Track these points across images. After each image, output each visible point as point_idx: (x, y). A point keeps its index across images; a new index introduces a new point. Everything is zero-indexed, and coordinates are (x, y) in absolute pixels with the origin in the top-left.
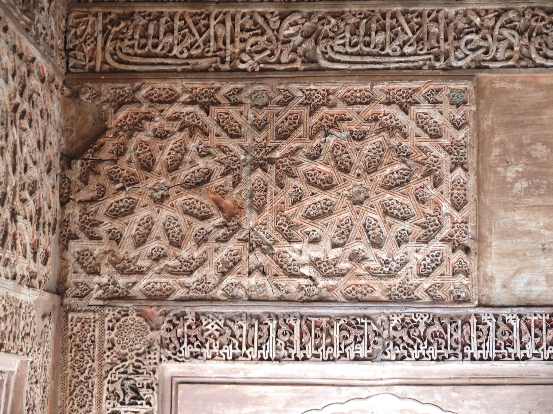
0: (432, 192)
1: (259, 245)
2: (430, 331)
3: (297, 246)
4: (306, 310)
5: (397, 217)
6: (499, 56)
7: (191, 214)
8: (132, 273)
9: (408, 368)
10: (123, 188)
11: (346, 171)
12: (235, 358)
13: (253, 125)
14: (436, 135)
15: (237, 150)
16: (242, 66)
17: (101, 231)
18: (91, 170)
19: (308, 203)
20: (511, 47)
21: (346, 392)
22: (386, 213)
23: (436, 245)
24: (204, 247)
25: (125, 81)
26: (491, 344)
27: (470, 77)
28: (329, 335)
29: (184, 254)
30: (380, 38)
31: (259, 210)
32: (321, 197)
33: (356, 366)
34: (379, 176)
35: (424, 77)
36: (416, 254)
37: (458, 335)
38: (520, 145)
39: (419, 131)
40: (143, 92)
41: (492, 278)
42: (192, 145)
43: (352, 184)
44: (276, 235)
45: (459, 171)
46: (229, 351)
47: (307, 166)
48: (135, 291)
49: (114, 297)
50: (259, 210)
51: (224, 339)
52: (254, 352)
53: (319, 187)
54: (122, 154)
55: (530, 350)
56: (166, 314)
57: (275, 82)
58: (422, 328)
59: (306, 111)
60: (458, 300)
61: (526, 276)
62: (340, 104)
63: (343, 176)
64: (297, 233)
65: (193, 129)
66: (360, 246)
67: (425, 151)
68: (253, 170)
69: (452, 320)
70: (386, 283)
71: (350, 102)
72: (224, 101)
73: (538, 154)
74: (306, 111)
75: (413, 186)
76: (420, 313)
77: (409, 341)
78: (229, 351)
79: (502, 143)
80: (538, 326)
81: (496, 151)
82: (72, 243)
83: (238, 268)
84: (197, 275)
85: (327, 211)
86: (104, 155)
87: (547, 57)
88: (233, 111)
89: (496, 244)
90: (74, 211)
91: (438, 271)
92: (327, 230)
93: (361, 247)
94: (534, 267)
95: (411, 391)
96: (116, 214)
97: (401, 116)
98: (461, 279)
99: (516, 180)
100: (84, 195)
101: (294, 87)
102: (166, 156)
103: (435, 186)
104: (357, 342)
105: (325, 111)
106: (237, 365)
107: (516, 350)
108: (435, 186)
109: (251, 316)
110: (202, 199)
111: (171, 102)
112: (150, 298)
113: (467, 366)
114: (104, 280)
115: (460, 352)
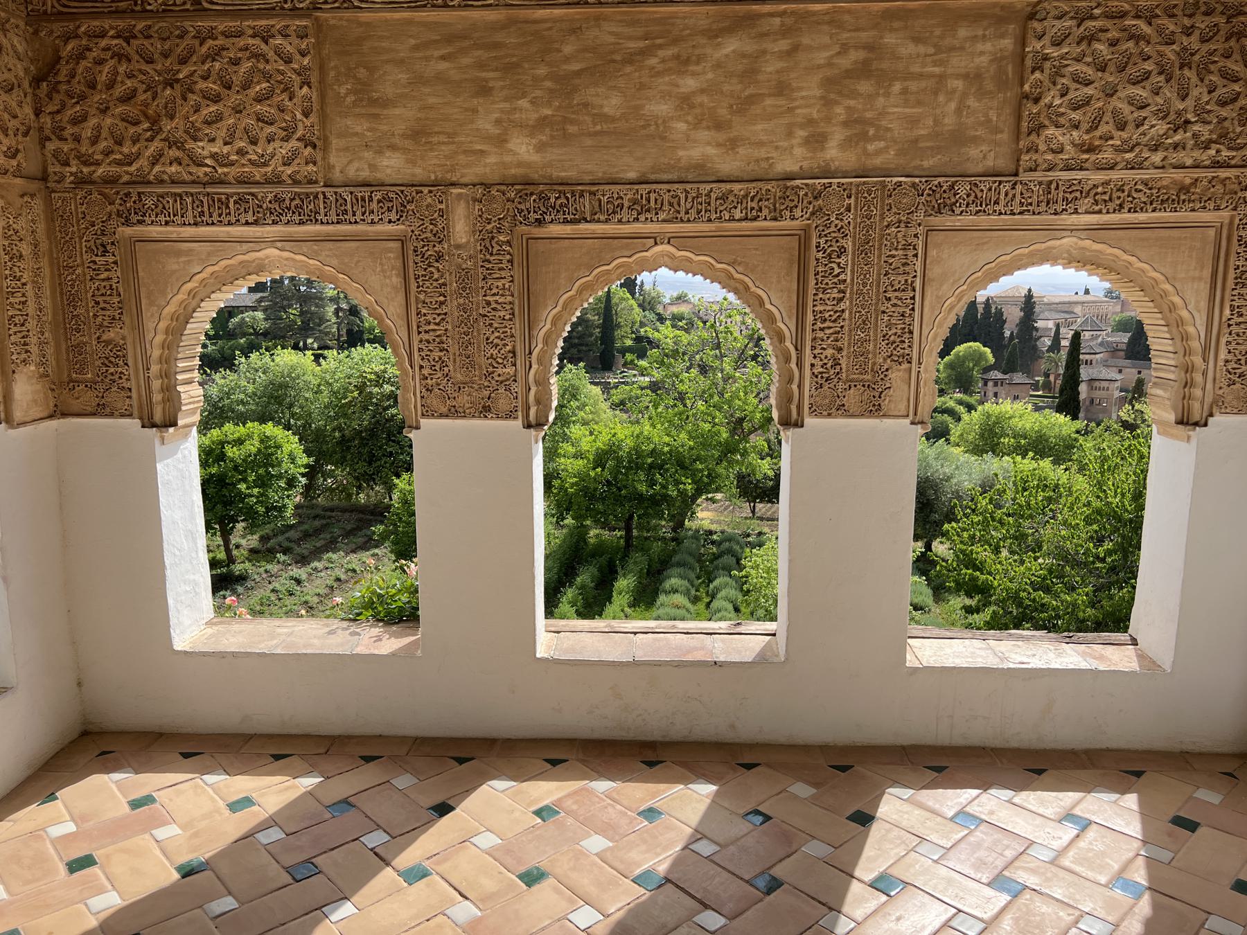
1: (175, 143)
2: (294, 203)
3: (201, 144)
5: (267, 123)
7: (127, 121)
8: (92, 164)
10: (77, 103)
11: (229, 88)
12: (167, 223)
13: (161, 54)
14: (288, 61)
16: (149, 8)
17: (66, 133)
18: (54, 89)
19: (205, 112)
21: (245, 247)
22: (258, 120)
23: (294, 143)
25: (69, 21)
26: (333, 212)
27: (309, 16)
28: (228, 207)
29: (126, 150)
31: (172, 118)
32: (213, 108)
33: (246, 228)
35: (277, 16)
36: (284, 150)
37: (312, 206)
38: (349, 69)
39: (277, 58)
40: (83, 29)
41: (334, 166)
42: (121, 69)
43: (234, 98)
44: (184, 135)
45: (305, 89)
46: (162, 219)
47: (202, 85)
49: (81, 182)
50: (172, 118)
51: (158, 210)
52: (178, 219)
53: (212, 100)
54: (73, 77)
55: (358, 217)
56: (118, 193)
57: (173, 20)
58: (287, 202)
59: (197, 42)
60: (310, 182)
61: (356, 165)
63: (227, 92)
64: (200, 134)
65: (121, 57)
67: (282, 73)
68: (165, 88)
69: (307, 195)
70: (263, 170)
71: (226, 35)
72: (139, 35)
74: (197, 42)
75: (276, 99)
76: (286, 191)
77: (278, 211)
79: (336, 67)
80: (363, 199)
81: (332, 74)
82: (47, 144)
85: (219, 118)
86: (61, 78)
89: (335, 142)
90: (46, 120)
93: (243, 144)
94: (360, 159)
95: (288, 245)
97: (263, 46)
98: (311, 167)
99: (347, 95)
100: (51, 108)
101: (187, 24)
102: (104, 78)
103: (290, 99)
104: (246, 212)
105: (210, 42)
106: (169, 228)
107: (349, 217)
108: (290, 99)
109: (175, 194)
111: (103, 37)
113: (318, 227)
114: (74, 169)
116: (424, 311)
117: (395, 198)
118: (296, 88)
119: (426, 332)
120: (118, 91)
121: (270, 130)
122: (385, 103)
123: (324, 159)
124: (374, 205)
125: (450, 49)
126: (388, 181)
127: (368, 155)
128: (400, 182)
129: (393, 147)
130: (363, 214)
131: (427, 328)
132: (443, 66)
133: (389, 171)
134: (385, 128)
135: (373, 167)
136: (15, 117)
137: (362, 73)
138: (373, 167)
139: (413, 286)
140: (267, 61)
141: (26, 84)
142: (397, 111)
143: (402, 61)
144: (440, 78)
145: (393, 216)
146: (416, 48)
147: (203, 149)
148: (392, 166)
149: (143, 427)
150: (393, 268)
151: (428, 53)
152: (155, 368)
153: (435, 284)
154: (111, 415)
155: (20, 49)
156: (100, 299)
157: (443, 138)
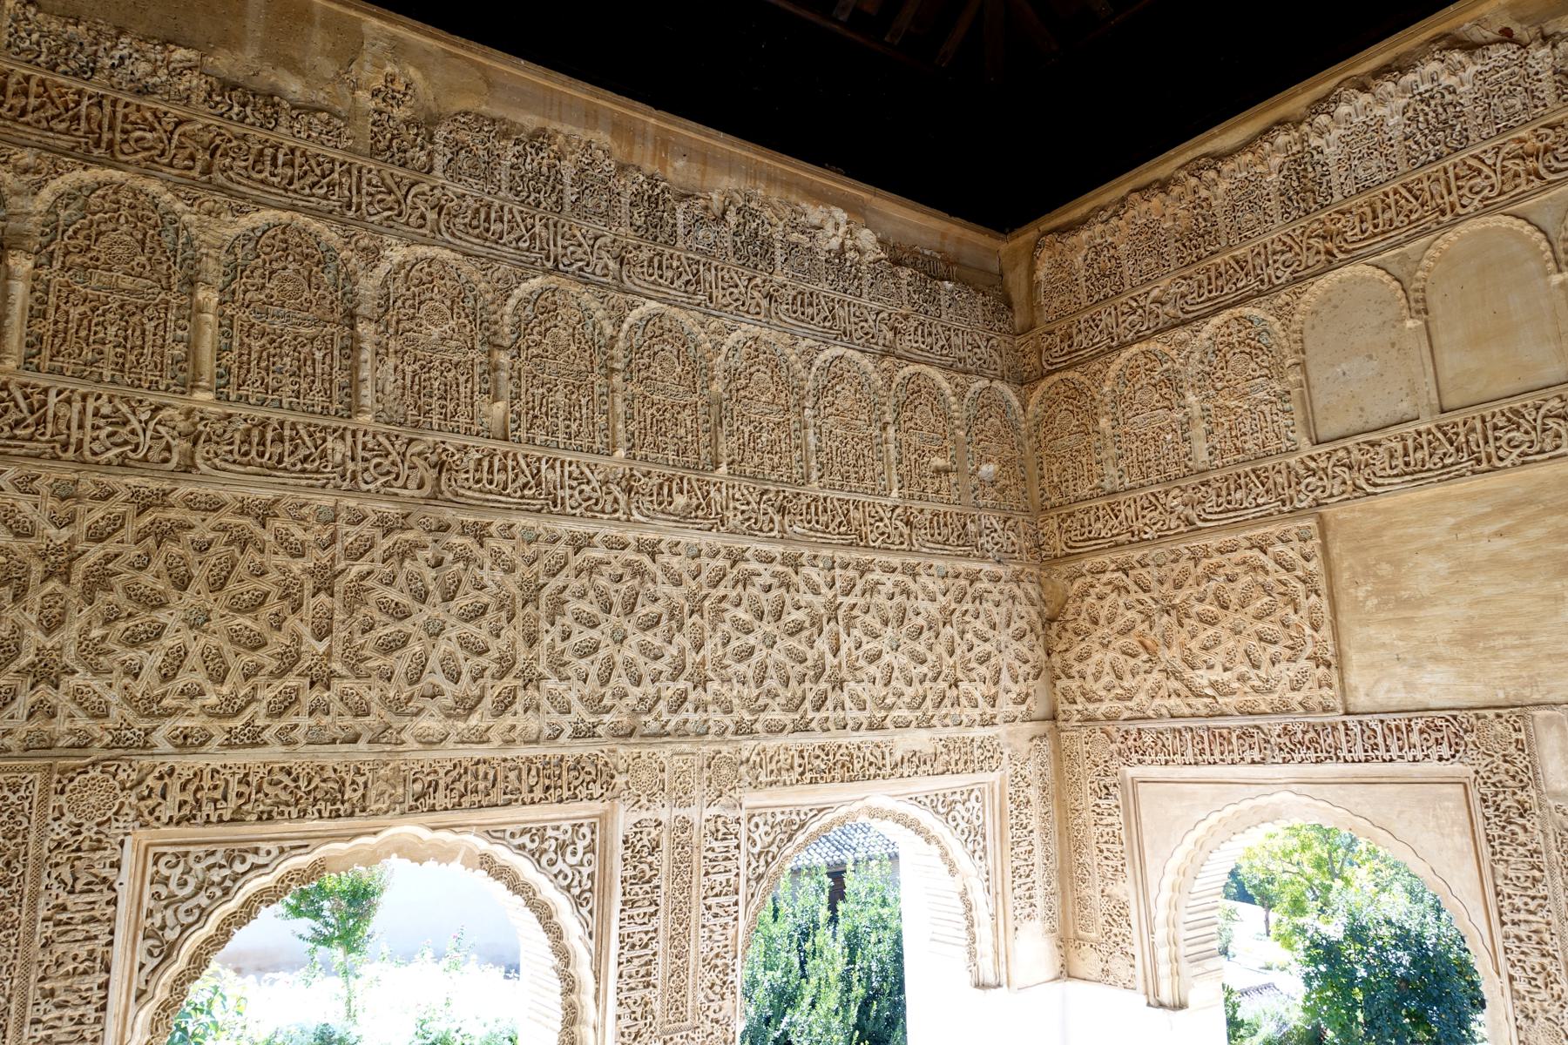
0: (1294, 618)
2: (1307, 737)
4: (1212, 723)
5: (1270, 642)
6: (1335, 492)
9: (1292, 770)
11: (1227, 608)
15: (1150, 602)
20: (1344, 483)
21: (1255, 790)
22: (1261, 639)
23: (1302, 663)
24: (1138, 678)
26: (1359, 747)
28: (1230, 743)
30: (1239, 495)
32: (1211, 631)
33: (1252, 767)
34: (1251, 610)
36: (1287, 672)
38: (1367, 567)
39: (1278, 567)
43: (1229, 619)
46: (1162, 757)
47: (1198, 608)
48: (1099, 715)
55: (1395, 752)
58: (1300, 735)
60: (1325, 710)
61: (1385, 684)
62: (1216, 555)
64: (1198, 662)
65: (1120, 589)
66: (1245, 669)
70: (1269, 698)
73: (1384, 573)
74: (1192, 563)
75: (1279, 614)
76: (1297, 721)
77: (1294, 746)
78: (1162, 757)
79: (1351, 567)
80: (1398, 728)
81: (1346, 575)
83: (1161, 693)
84: (1136, 700)
85: (1217, 641)
87: (1375, 485)
88: (1143, 571)
89: (1354, 658)
90: (1056, 659)
91: (1307, 685)
92: (1218, 658)
95: (1305, 788)
96: (1080, 659)
97: (1262, 556)
98: (1325, 691)
99: (1366, 598)
100: (1061, 647)
105: (1205, 562)
106: (1169, 768)
110: (1132, 641)
112: (1109, 719)
114: (1080, 707)
115: (1333, 755)
116: (1507, 890)
117: (1447, 729)
118: (1302, 599)
119: (1514, 923)
120: (1119, 623)
121: (1272, 649)
122: (1420, 603)
123: (1342, 680)
124: (1415, 738)
125: (1508, 522)
126: (1434, 704)
127: (1400, 670)
128: (1448, 705)
129: (1436, 658)
130: (1401, 749)
131: (1516, 917)
132: (1499, 544)
133: (1433, 690)
134: (1421, 634)
135: (1409, 686)
136: (1026, 662)
137: (1385, 569)
138: (1409, 686)
139: (1486, 851)
140: (1267, 573)
141: (1039, 627)
142: (1438, 611)
143: (1439, 547)
144: (1496, 561)
145: (1446, 753)
146: (1457, 528)
147: (1202, 678)
148: (1438, 686)
149: (1149, 1004)
150: (1454, 823)
151: (1476, 531)
152: (1161, 934)
153: (1521, 850)
154: (1114, 984)
155: (1034, 595)
156: (1104, 847)
157: (1510, 640)
